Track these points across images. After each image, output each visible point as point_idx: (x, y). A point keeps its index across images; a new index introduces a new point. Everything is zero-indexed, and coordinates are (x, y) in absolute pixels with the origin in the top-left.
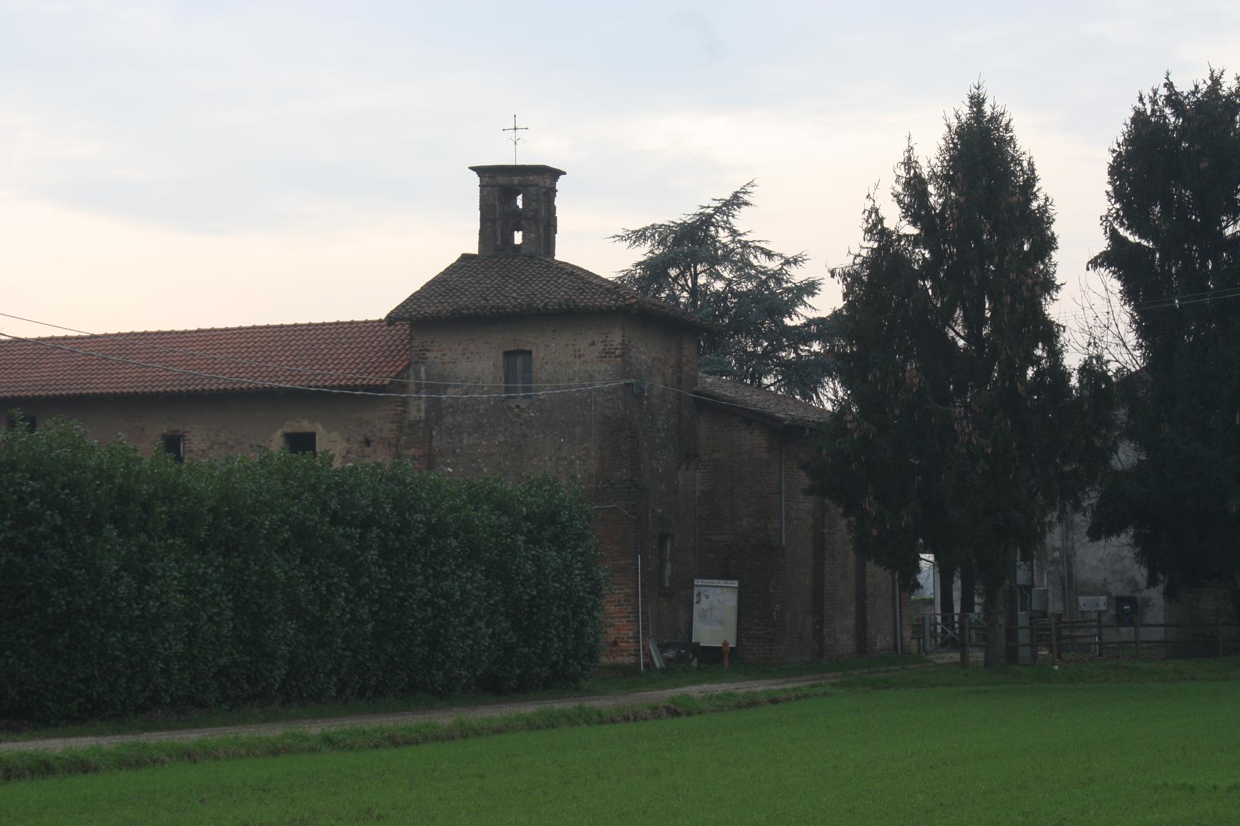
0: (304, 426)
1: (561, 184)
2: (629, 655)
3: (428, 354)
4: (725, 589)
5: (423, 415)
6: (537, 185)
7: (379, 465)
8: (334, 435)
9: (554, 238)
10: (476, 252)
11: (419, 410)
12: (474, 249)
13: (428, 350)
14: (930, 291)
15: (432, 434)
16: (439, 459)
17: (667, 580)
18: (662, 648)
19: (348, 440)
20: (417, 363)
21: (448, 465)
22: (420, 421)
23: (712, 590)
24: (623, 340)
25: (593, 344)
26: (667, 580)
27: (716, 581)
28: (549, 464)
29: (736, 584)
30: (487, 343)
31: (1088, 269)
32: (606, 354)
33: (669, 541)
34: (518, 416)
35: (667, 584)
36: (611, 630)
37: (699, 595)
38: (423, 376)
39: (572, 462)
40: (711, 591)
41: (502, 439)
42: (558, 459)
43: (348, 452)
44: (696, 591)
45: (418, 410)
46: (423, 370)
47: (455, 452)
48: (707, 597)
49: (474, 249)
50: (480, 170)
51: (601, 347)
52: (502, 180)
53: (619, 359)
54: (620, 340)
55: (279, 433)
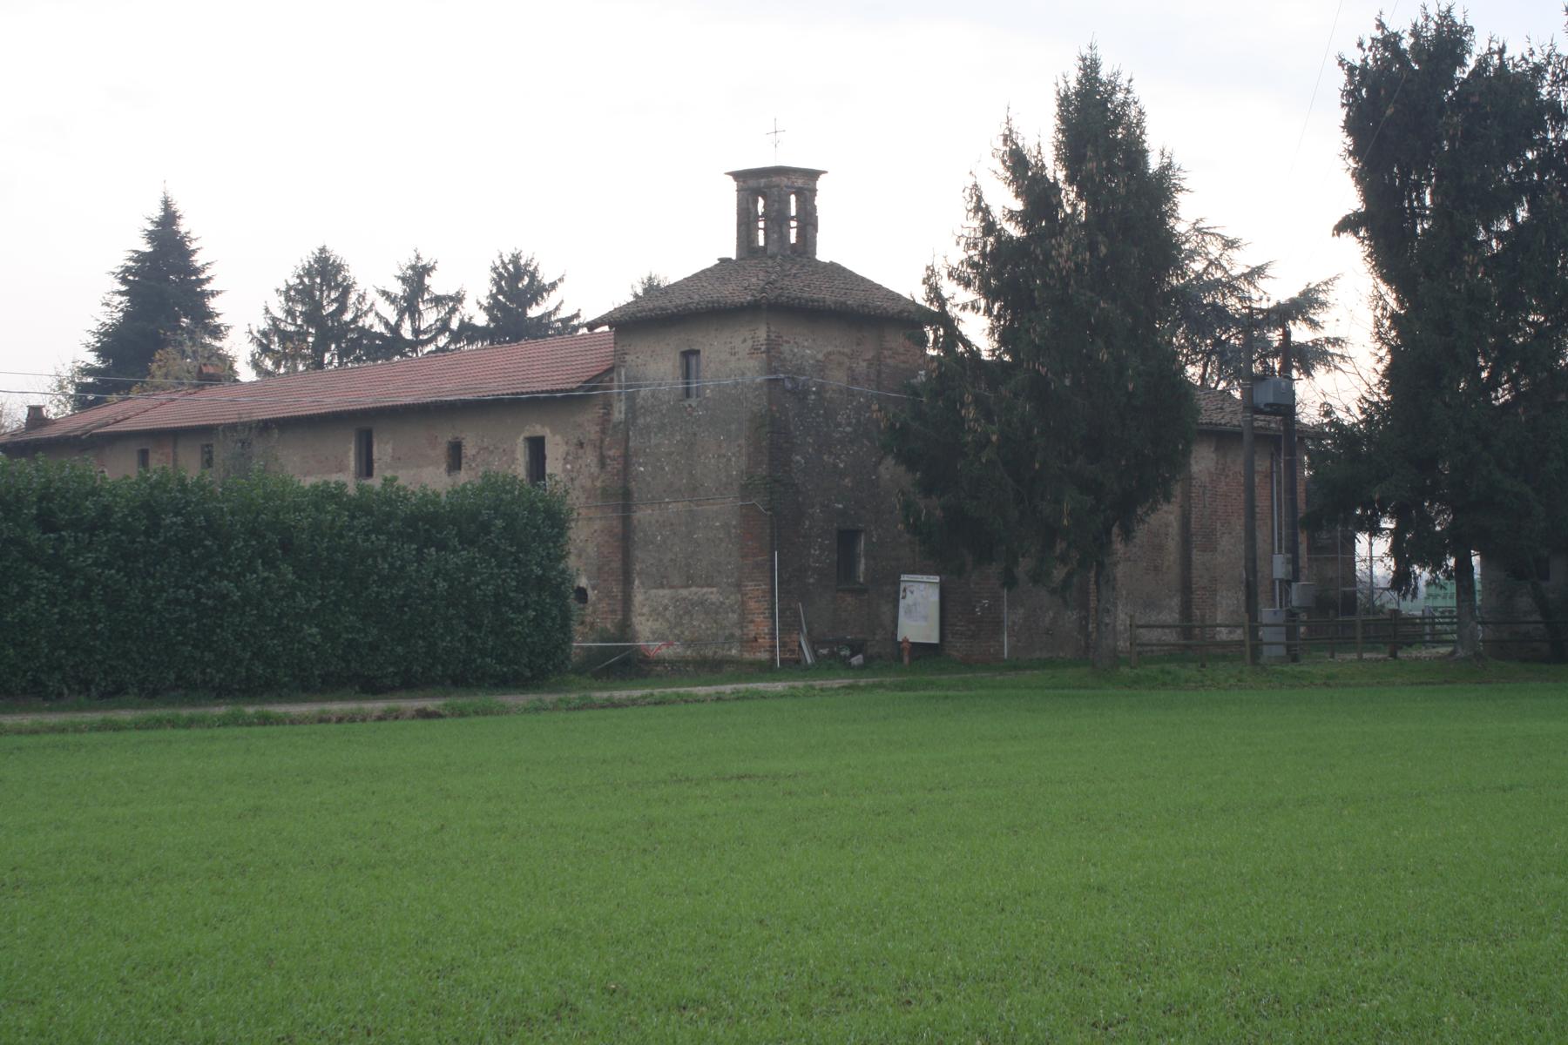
0: (538, 430)
1: (821, 184)
2: (765, 651)
3: (627, 357)
4: (928, 585)
5: (623, 416)
6: (778, 186)
7: (127, 477)
8: (558, 438)
9: (815, 237)
10: (734, 257)
11: (620, 412)
12: (732, 254)
13: (626, 354)
14: (194, 278)
15: (628, 435)
16: (634, 459)
17: (862, 576)
18: (815, 644)
19: (567, 443)
20: (619, 366)
21: (640, 465)
22: (621, 423)
23: (916, 585)
24: (768, 336)
25: (745, 341)
26: (862, 576)
27: (920, 576)
28: (712, 461)
29: (937, 579)
30: (668, 344)
31: (1333, 235)
32: (755, 350)
33: (863, 537)
34: (690, 415)
35: (862, 580)
36: (751, 627)
37: (905, 590)
38: (623, 378)
39: (729, 460)
40: (915, 587)
41: (679, 438)
42: (719, 456)
43: (567, 454)
44: (902, 586)
45: (619, 413)
46: (623, 373)
47: (645, 451)
48: (912, 592)
49: (732, 254)
50: (737, 175)
51: (750, 343)
52: (752, 183)
53: (764, 355)
54: (764, 336)
55: (521, 438)
